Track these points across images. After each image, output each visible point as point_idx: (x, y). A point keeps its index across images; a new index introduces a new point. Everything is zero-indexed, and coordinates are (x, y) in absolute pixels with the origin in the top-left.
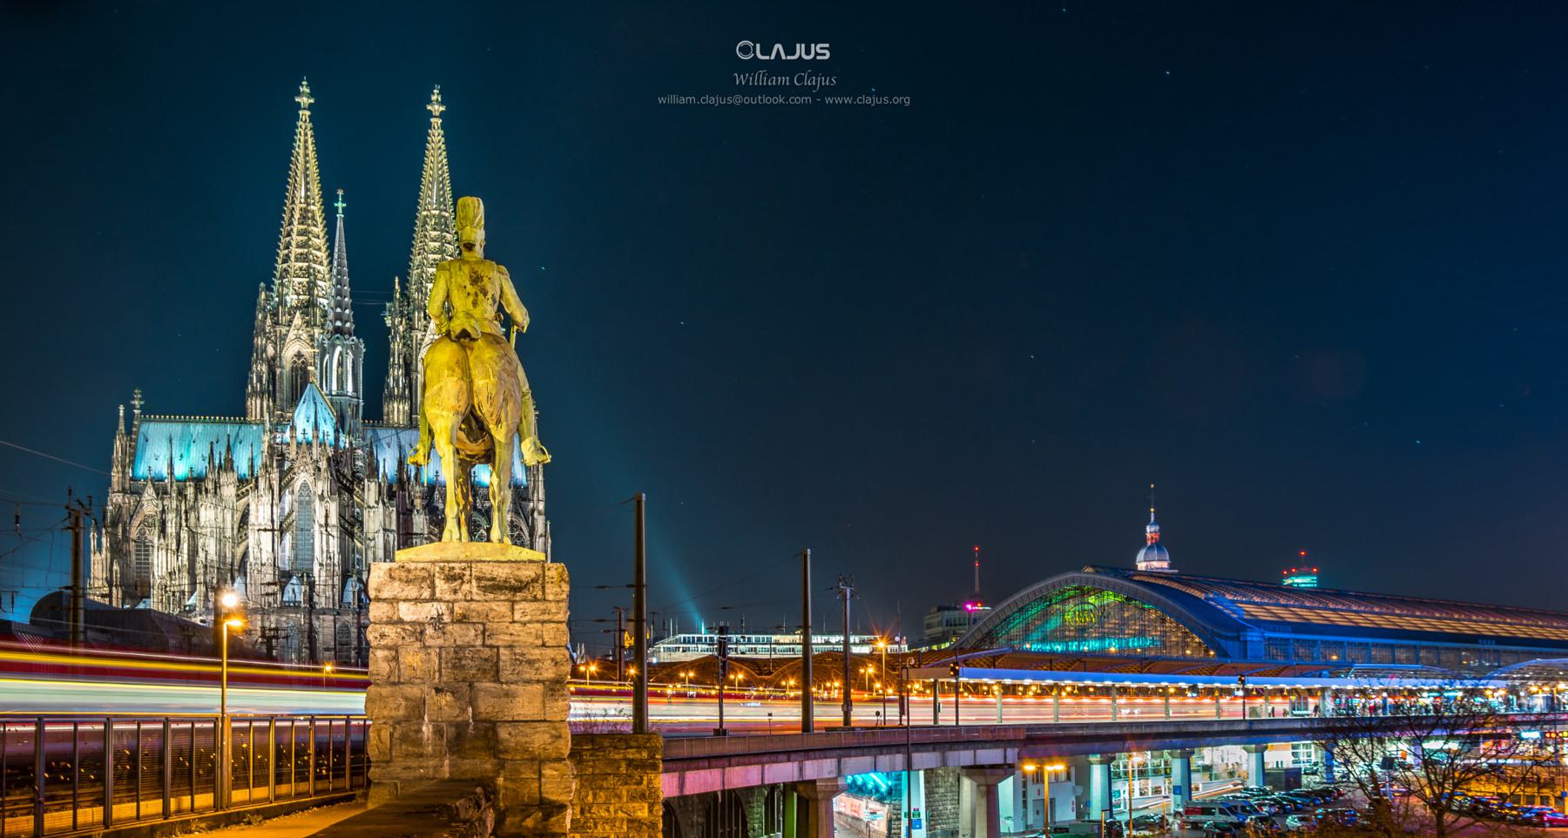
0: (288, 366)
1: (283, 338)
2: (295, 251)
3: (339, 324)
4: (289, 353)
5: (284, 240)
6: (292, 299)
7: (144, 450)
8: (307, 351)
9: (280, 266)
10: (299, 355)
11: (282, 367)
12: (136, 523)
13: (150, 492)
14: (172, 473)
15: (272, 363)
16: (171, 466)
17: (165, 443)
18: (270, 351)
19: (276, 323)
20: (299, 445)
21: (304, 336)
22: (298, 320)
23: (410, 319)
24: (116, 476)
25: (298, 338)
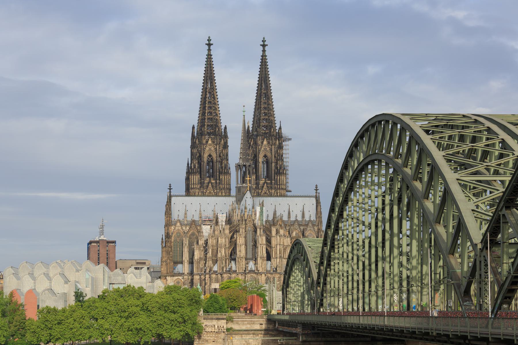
21: (213, 149)
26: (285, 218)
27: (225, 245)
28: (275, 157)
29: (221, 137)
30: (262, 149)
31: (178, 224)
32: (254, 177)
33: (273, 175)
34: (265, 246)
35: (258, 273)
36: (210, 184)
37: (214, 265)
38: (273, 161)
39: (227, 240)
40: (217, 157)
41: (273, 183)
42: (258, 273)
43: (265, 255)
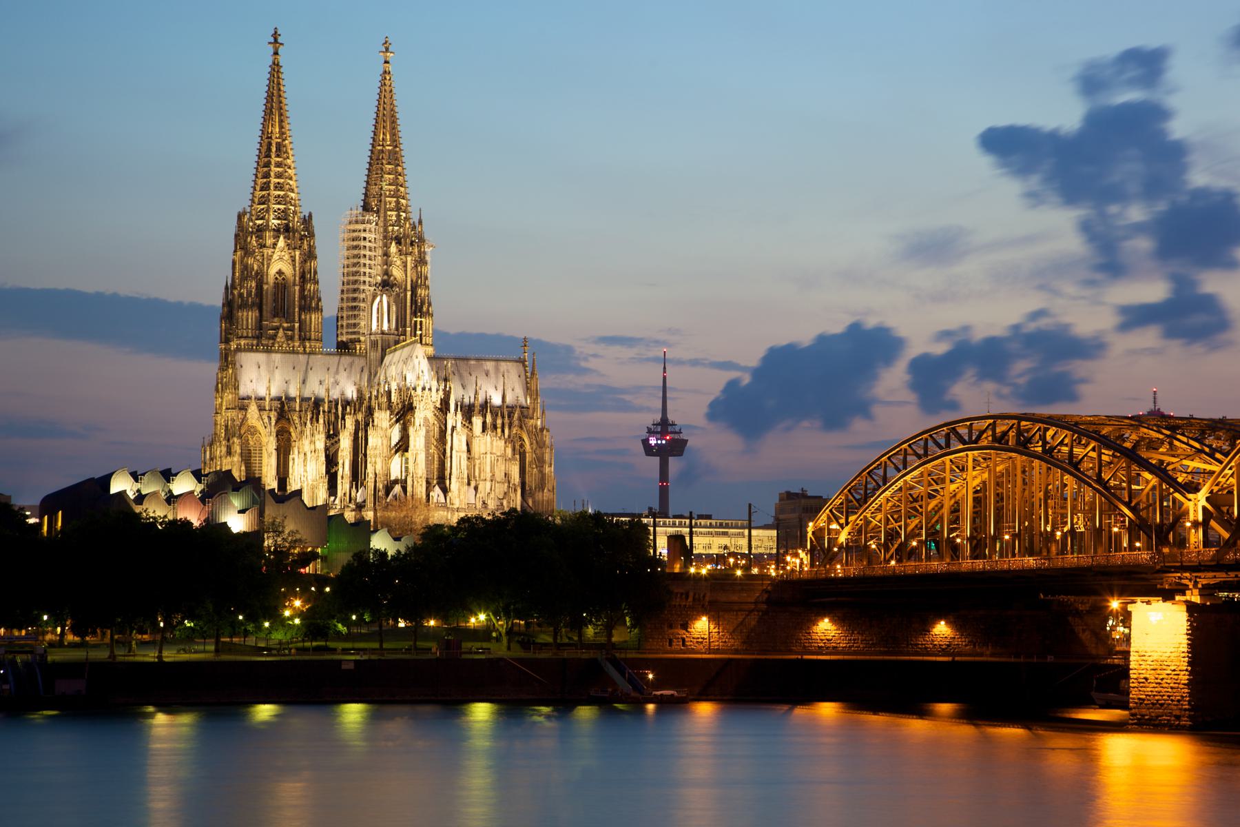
0: (271, 280)
1: (270, 258)
2: (274, 180)
4: (273, 271)
8: (288, 270)
10: (280, 272)
13: (253, 409)
15: (260, 278)
16: (269, 389)
17: (255, 368)
18: (256, 267)
19: (263, 246)
20: (424, 389)
21: (287, 257)
22: (281, 242)
25: (281, 258)
29: (300, 233)
31: (253, 409)
40: (295, 275)
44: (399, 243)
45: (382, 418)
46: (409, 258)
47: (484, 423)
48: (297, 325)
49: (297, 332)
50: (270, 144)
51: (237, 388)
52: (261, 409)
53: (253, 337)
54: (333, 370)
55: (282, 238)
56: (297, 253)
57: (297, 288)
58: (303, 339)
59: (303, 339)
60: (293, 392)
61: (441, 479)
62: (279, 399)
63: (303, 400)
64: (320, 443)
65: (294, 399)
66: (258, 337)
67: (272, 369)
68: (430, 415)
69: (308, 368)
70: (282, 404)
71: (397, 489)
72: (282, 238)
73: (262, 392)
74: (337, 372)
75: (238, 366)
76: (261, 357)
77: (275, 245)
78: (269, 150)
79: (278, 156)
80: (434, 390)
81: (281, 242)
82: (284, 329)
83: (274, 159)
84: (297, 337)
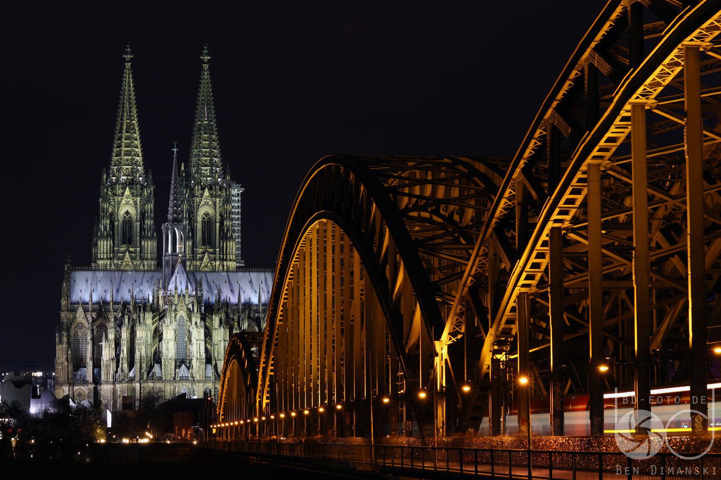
0: (121, 219)
1: (119, 204)
2: (124, 149)
3: (175, 216)
4: (122, 212)
5: (117, 142)
6: (123, 178)
7: (74, 287)
8: (132, 211)
9: (115, 158)
10: (127, 213)
11: (118, 221)
12: (73, 326)
13: (80, 310)
14: (92, 300)
15: (112, 217)
16: (91, 296)
17: (84, 282)
18: (110, 210)
19: (114, 195)
20: (179, 296)
21: (131, 202)
22: (127, 192)
23: (192, 189)
24: (63, 302)
25: (127, 203)
26: (234, 300)
27: (147, 341)
28: (221, 215)
30: (202, 202)
31: (80, 310)
32: (190, 244)
33: (217, 241)
34: (203, 343)
35: (193, 381)
36: (127, 253)
37: (130, 371)
38: (218, 220)
39: (149, 334)
40: (137, 215)
41: (218, 253)
42: (193, 381)
43: (204, 356)
44: (210, 189)
45: (149, 316)
46: (218, 200)
47: (221, 320)
48: (138, 249)
49: (138, 254)
50: (122, 124)
51: (69, 296)
52: (86, 311)
53: (107, 258)
54: (138, 282)
55: (127, 189)
56: (138, 199)
57: (138, 223)
58: (142, 259)
59: (142, 259)
60: (109, 298)
61: (183, 361)
62: (98, 303)
63: (115, 303)
64: (111, 336)
65: (109, 303)
66: (111, 259)
67: (96, 281)
68: (182, 313)
69: (121, 281)
70: (100, 306)
71: (157, 366)
72: (127, 189)
73: (87, 299)
74: (141, 284)
75: (72, 281)
76: (89, 274)
77: (123, 193)
78: (122, 128)
79: (127, 132)
80: (187, 296)
81: (127, 192)
82: (130, 252)
83: (124, 135)
84: (138, 257)
